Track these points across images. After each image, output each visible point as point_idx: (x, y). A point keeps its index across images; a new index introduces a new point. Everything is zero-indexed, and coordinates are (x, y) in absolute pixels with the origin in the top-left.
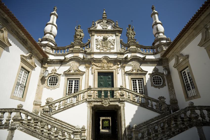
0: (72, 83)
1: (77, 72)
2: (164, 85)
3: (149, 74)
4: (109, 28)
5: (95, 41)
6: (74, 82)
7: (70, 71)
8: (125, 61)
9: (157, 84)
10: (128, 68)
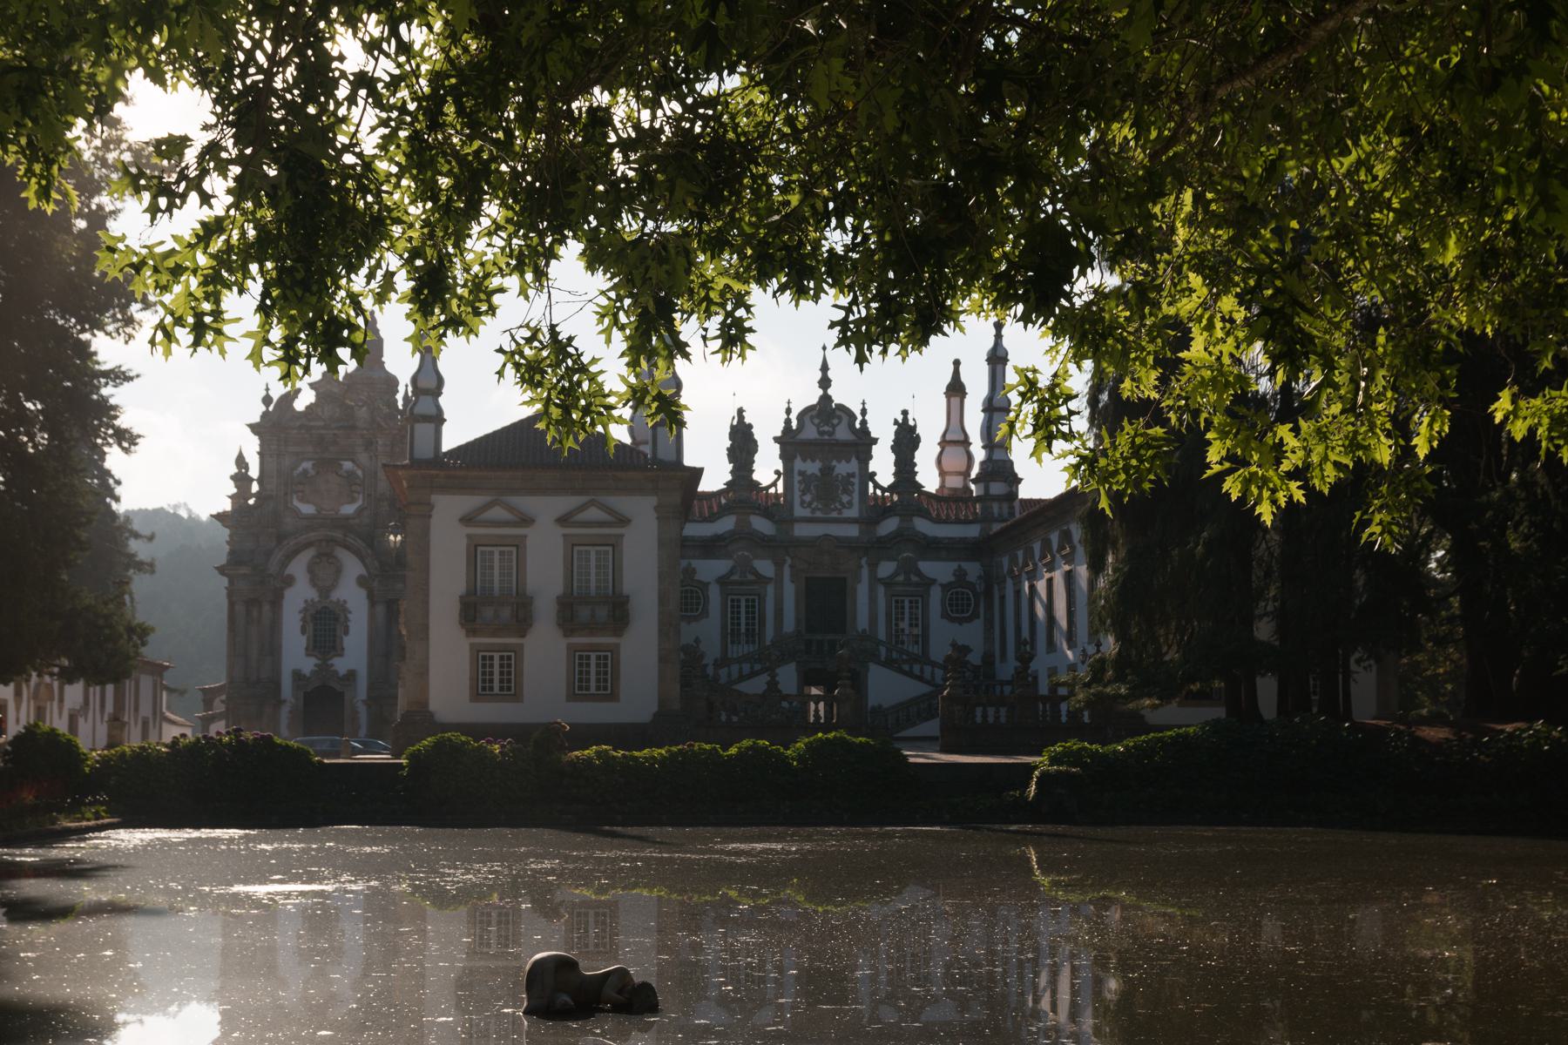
0: (739, 607)
1: (751, 577)
2: (975, 615)
3: (941, 585)
4: (842, 434)
5: (797, 478)
6: (743, 604)
7: (731, 572)
8: (879, 548)
9: (957, 612)
10: (886, 569)
